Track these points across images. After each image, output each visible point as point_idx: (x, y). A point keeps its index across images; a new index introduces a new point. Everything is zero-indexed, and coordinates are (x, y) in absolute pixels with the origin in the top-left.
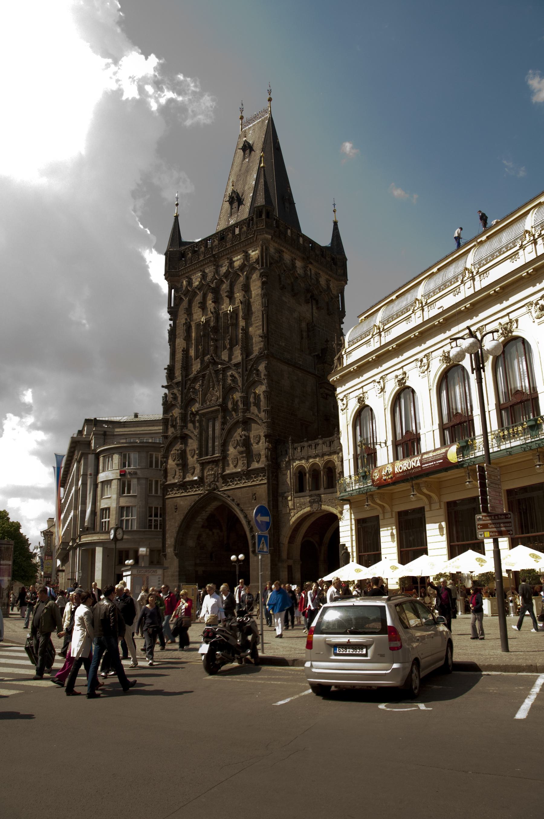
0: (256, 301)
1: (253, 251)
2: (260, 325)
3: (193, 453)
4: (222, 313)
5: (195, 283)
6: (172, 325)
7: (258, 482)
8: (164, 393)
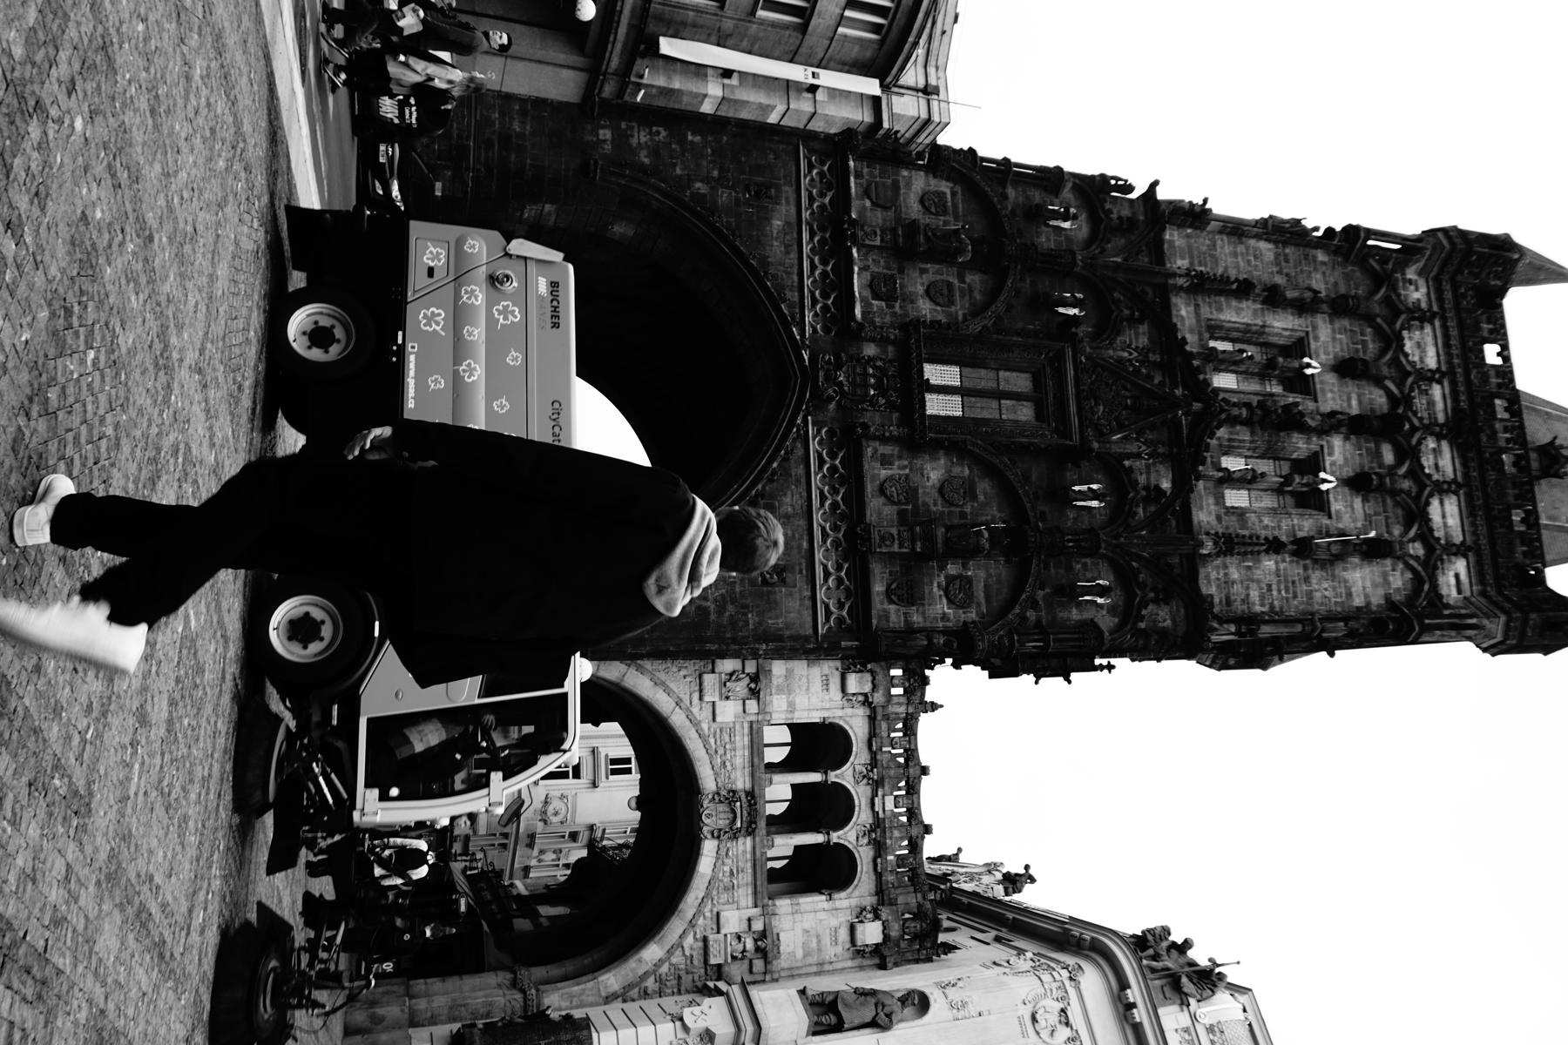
0: (1334, 588)
1: (1457, 576)
2: (1272, 605)
3: (940, 300)
4: (1322, 447)
5: (1410, 338)
6: (1315, 234)
7: (821, 594)
8: (1134, 184)
